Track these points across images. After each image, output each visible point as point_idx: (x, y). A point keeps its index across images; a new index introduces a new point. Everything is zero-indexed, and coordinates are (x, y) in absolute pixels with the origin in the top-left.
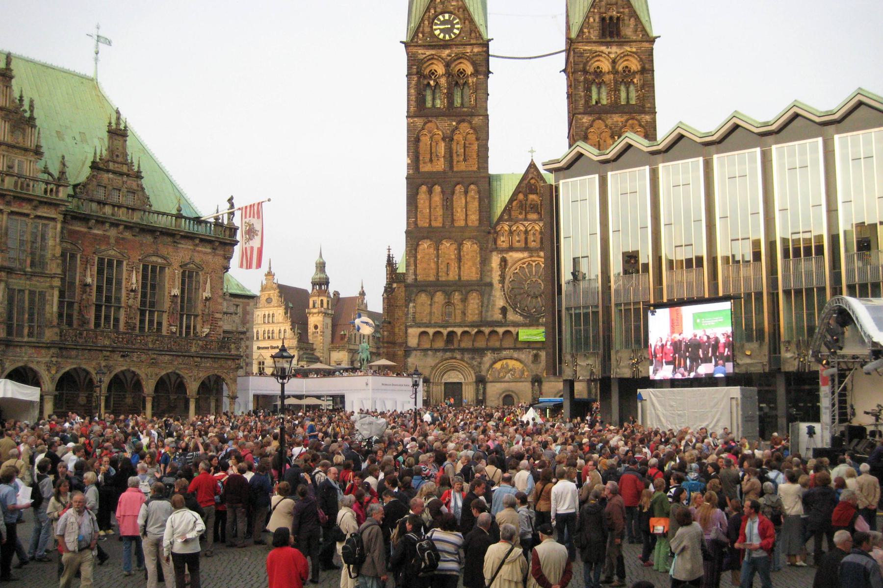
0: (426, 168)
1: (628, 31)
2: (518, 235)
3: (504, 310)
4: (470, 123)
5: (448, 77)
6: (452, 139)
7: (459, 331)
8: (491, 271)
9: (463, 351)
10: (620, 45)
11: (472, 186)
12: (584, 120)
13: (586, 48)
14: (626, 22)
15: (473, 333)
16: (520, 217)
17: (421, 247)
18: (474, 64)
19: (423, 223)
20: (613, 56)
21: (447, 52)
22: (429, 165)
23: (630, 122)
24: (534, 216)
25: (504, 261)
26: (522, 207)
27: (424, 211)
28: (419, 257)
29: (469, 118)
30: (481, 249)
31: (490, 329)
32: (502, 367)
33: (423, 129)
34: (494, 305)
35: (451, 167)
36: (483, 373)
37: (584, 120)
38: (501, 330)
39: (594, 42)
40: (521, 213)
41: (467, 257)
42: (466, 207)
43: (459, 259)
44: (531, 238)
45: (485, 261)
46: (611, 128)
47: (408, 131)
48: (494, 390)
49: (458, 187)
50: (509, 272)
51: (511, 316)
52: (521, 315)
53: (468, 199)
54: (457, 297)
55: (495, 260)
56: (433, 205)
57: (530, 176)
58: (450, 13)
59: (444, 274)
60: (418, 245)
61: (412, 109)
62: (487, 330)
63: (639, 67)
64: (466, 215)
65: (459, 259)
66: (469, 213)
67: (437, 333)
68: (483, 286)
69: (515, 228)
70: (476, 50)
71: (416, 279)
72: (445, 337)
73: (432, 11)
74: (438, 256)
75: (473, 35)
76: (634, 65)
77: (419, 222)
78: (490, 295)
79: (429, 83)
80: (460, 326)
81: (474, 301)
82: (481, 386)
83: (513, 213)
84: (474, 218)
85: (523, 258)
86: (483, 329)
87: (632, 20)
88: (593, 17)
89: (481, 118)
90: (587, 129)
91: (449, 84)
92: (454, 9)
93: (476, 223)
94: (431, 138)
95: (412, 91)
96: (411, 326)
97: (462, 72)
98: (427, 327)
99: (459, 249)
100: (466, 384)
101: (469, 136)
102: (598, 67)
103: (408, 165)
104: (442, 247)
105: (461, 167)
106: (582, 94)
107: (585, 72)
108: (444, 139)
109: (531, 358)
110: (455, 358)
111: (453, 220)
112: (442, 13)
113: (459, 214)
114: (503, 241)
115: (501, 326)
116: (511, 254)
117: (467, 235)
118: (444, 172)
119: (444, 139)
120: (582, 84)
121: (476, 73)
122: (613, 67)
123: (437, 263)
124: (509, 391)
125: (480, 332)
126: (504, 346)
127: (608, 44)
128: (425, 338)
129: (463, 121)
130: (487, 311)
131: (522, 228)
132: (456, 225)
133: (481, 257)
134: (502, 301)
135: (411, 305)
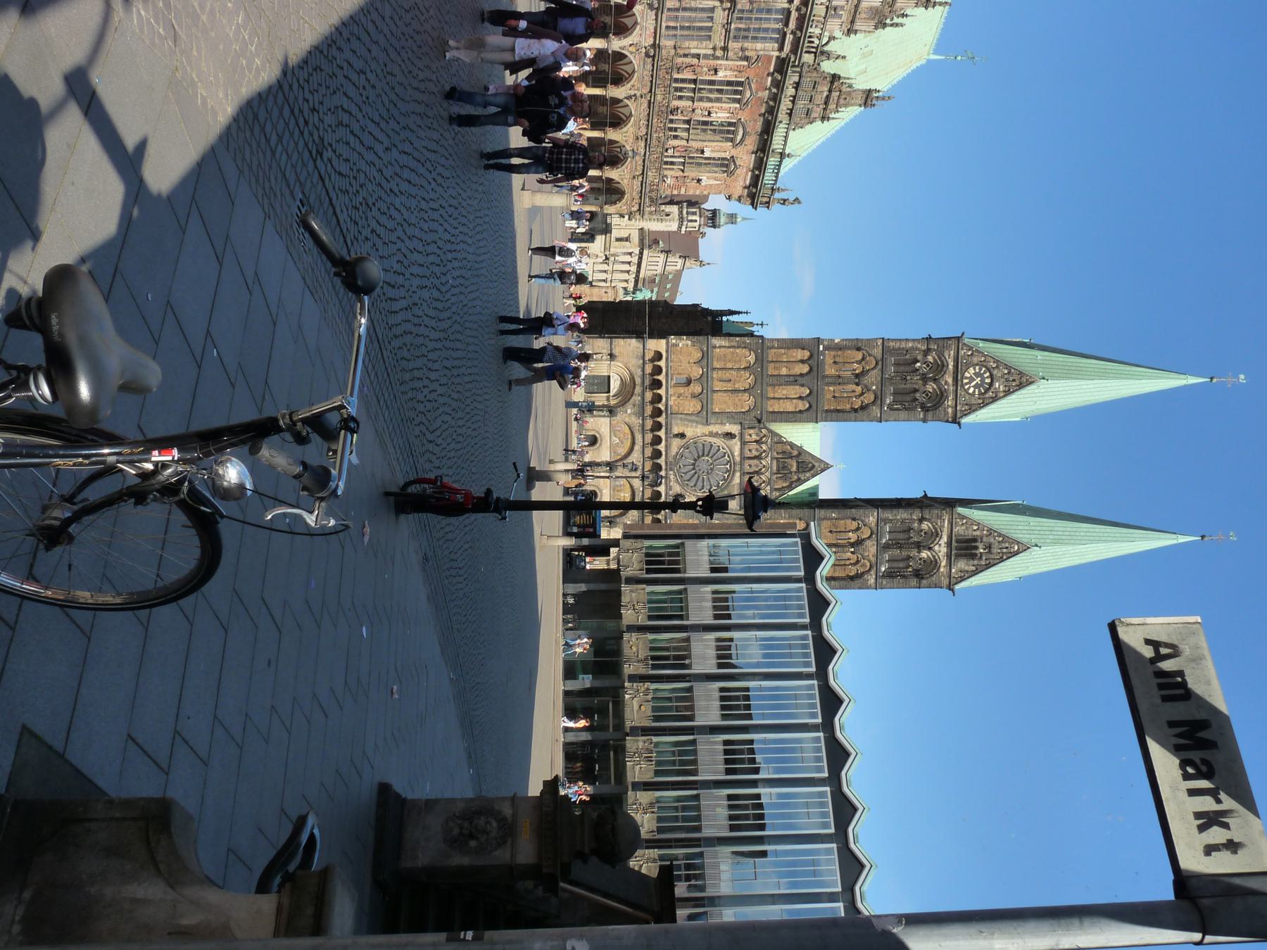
1: (962, 564)
7: (662, 392)
10: (947, 556)
12: (871, 518)
13: (946, 522)
14: (971, 562)
15: (660, 406)
19: (772, 355)
21: (950, 380)
22: (832, 361)
23: (868, 564)
25: (730, 436)
27: (785, 356)
28: (738, 351)
29: (879, 402)
35: (829, 384)
37: (871, 518)
38: (662, 434)
40: (777, 453)
41: (737, 399)
42: (787, 398)
51: (676, 443)
52: (677, 453)
53: (794, 401)
55: (735, 429)
56: (789, 365)
57: (816, 464)
58: (991, 384)
59: (720, 376)
61: (892, 344)
66: (781, 401)
68: (705, 414)
69: (764, 448)
71: (715, 347)
72: (656, 377)
74: (739, 369)
75: (967, 407)
77: (773, 351)
78: (697, 422)
79: (918, 361)
81: (693, 406)
83: (779, 445)
84: (776, 407)
85: (733, 456)
87: (974, 568)
88: (978, 529)
89: (879, 415)
92: (995, 388)
93: (771, 410)
95: (910, 345)
100: (608, 399)
106: (899, 517)
111: (773, 385)
112: (991, 376)
113: (783, 391)
114: (752, 435)
115: (666, 433)
116: (739, 443)
117: (759, 400)
120: (909, 517)
124: (601, 441)
126: (646, 435)
127: (949, 544)
130: (681, 419)
132: (769, 388)
134: (692, 434)
135: (689, 343)
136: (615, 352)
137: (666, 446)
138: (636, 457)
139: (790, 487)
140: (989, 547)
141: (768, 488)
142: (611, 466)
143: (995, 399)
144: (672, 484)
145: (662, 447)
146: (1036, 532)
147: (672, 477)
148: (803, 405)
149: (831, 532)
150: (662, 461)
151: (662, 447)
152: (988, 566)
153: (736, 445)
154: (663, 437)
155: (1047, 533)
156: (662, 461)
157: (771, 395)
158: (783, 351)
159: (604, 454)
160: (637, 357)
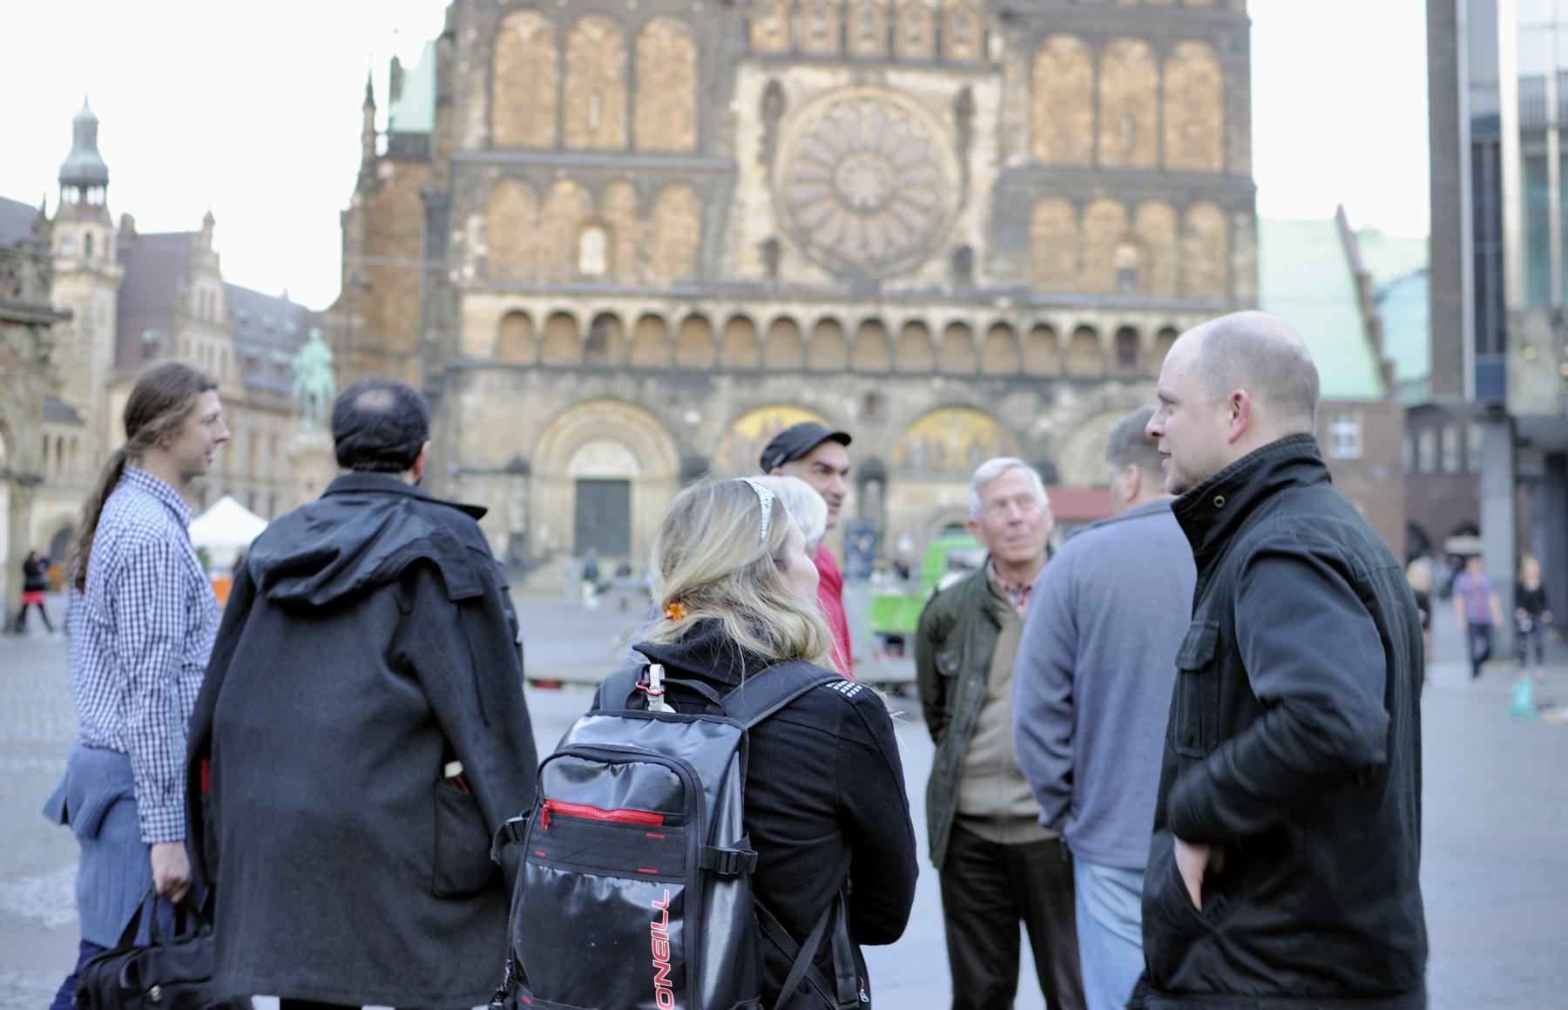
3: (771, 250)
7: (630, 311)
8: (733, 122)
9: (638, 374)
28: (501, 67)
34: (739, 235)
38: (764, 313)
43: (631, 79)
44: (858, 27)
50: (792, 131)
51: (792, 270)
54: (621, 199)
55: (749, 85)
60: (498, 29)
65: (631, 79)
67: (562, 317)
74: (563, 67)
80: (628, 295)
86: (707, 307)
96: (476, 291)
98: (527, 293)
99: (631, 48)
100: (652, 483)
104: (576, 39)
123: (560, 88)
125: (697, 318)
130: (719, 251)
135: (474, 222)
136: (501, 458)
145: (806, 314)
147: (900, 285)
150: (850, 315)
151: (806, 314)
153: (800, 79)
156: (850, 315)
160: (520, 388)
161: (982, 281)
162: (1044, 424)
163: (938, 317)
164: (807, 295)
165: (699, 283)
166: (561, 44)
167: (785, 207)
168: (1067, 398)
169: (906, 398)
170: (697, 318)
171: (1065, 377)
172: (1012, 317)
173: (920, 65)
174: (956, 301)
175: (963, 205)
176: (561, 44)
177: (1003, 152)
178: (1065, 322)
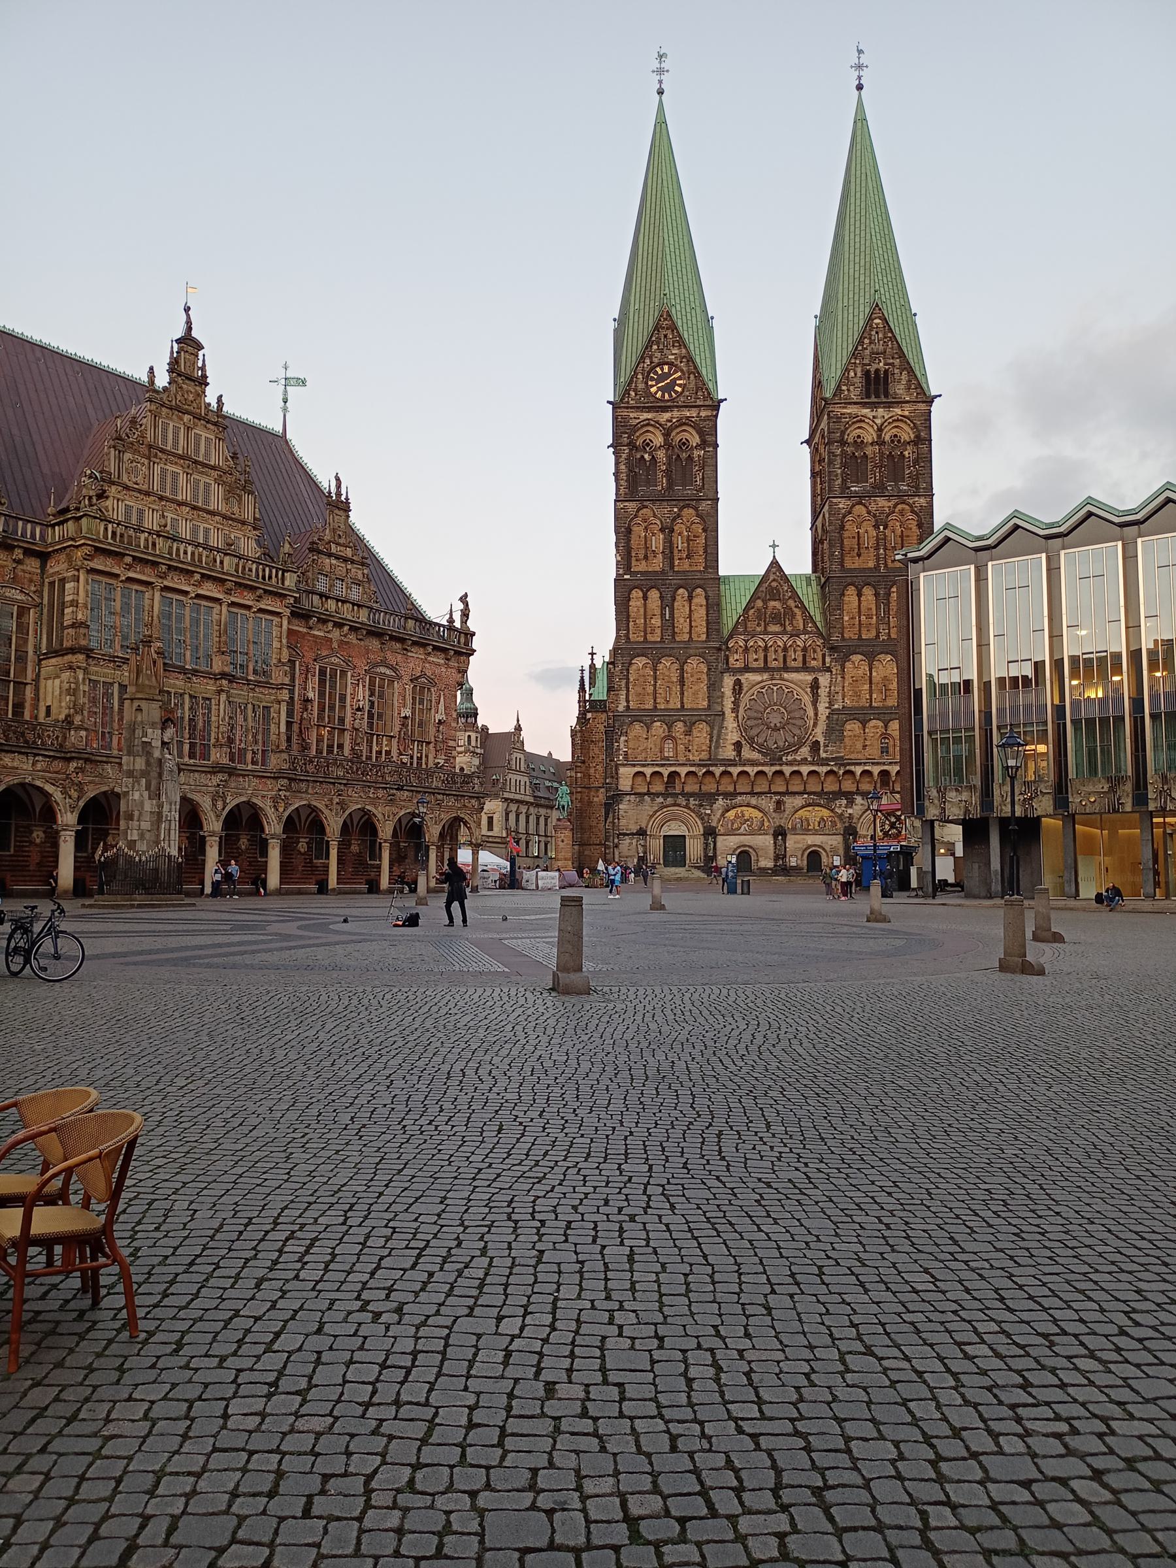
0: (640, 567)
1: (899, 389)
2: (756, 652)
4: (696, 509)
5: (667, 450)
6: (672, 531)
7: (683, 771)
11: (699, 590)
15: (700, 774)
16: (758, 629)
17: (634, 667)
18: (701, 433)
20: (878, 421)
21: (667, 415)
23: (900, 507)
24: (776, 628)
25: (738, 686)
26: (760, 615)
30: (709, 669)
31: (722, 769)
32: (736, 816)
33: (636, 516)
35: (672, 566)
36: (714, 824)
38: (735, 771)
39: (855, 403)
40: (759, 625)
42: (690, 617)
43: (682, 682)
45: (714, 686)
46: (875, 516)
47: (616, 519)
48: (727, 845)
49: (681, 591)
50: (745, 700)
51: (747, 753)
52: (759, 752)
55: (728, 681)
56: (649, 613)
60: (630, 664)
62: (718, 771)
63: (912, 436)
64: (691, 627)
65: (682, 682)
67: (655, 773)
68: (714, 718)
70: (703, 414)
71: (628, 707)
73: (648, 361)
74: (655, 679)
76: (907, 434)
81: (701, 733)
82: (710, 839)
83: (749, 625)
90: (844, 517)
91: (669, 458)
92: (676, 359)
93: (704, 637)
94: (646, 529)
97: (684, 444)
98: (644, 766)
99: (682, 670)
101: (693, 526)
102: (859, 437)
103: (618, 562)
104: (660, 666)
105: (685, 566)
106: (839, 471)
107: (843, 443)
108: (662, 530)
109: (772, 806)
110: (679, 805)
112: (660, 365)
113: (682, 624)
114: (736, 660)
115: (735, 765)
118: (663, 572)
119: (662, 530)
121: (703, 444)
122: (879, 436)
123: (655, 686)
124: (745, 846)
125: (709, 773)
127: (874, 406)
128: (639, 779)
129: (688, 506)
130: (717, 747)
131: (761, 643)
132: (677, 639)
133: (709, 679)
135: (623, 738)
136: (634, 828)
137: (752, 765)
138: (768, 804)
139: (804, 609)
140: (875, 355)
141: (802, 637)
142: (780, 833)
143: (690, 359)
144: (799, 758)
146: (856, 298)
147: (790, 758)
148: (700, 599)
149: (859, 555)
152: (902, 355)
154: (740, 769)
155: (857, 283)
157: (686, 637)
158: (631, 624)
159: (765, 842)
161: (823, 755)
162: (850, 811)
163: (805, 770)
164: (753, 763)
165: (710, 759)
166: (655, 670)
167: (743, 728)
168: (859, 799)
169: (791, 802)
170: (709, 773)
171: (858, 792)
172: (835, 769)
173: (797, 670)
174: (812, 763)
175: (815, 725)
176: (655, 670)
177: (831, 703)
178: (858, 770)
